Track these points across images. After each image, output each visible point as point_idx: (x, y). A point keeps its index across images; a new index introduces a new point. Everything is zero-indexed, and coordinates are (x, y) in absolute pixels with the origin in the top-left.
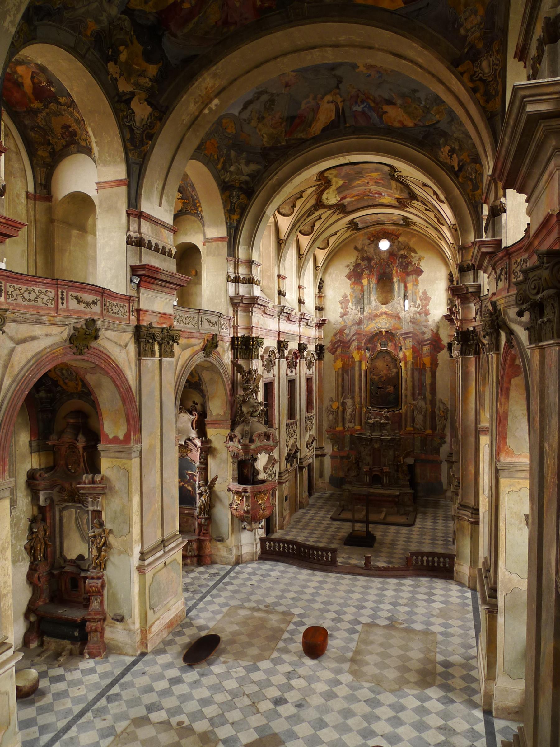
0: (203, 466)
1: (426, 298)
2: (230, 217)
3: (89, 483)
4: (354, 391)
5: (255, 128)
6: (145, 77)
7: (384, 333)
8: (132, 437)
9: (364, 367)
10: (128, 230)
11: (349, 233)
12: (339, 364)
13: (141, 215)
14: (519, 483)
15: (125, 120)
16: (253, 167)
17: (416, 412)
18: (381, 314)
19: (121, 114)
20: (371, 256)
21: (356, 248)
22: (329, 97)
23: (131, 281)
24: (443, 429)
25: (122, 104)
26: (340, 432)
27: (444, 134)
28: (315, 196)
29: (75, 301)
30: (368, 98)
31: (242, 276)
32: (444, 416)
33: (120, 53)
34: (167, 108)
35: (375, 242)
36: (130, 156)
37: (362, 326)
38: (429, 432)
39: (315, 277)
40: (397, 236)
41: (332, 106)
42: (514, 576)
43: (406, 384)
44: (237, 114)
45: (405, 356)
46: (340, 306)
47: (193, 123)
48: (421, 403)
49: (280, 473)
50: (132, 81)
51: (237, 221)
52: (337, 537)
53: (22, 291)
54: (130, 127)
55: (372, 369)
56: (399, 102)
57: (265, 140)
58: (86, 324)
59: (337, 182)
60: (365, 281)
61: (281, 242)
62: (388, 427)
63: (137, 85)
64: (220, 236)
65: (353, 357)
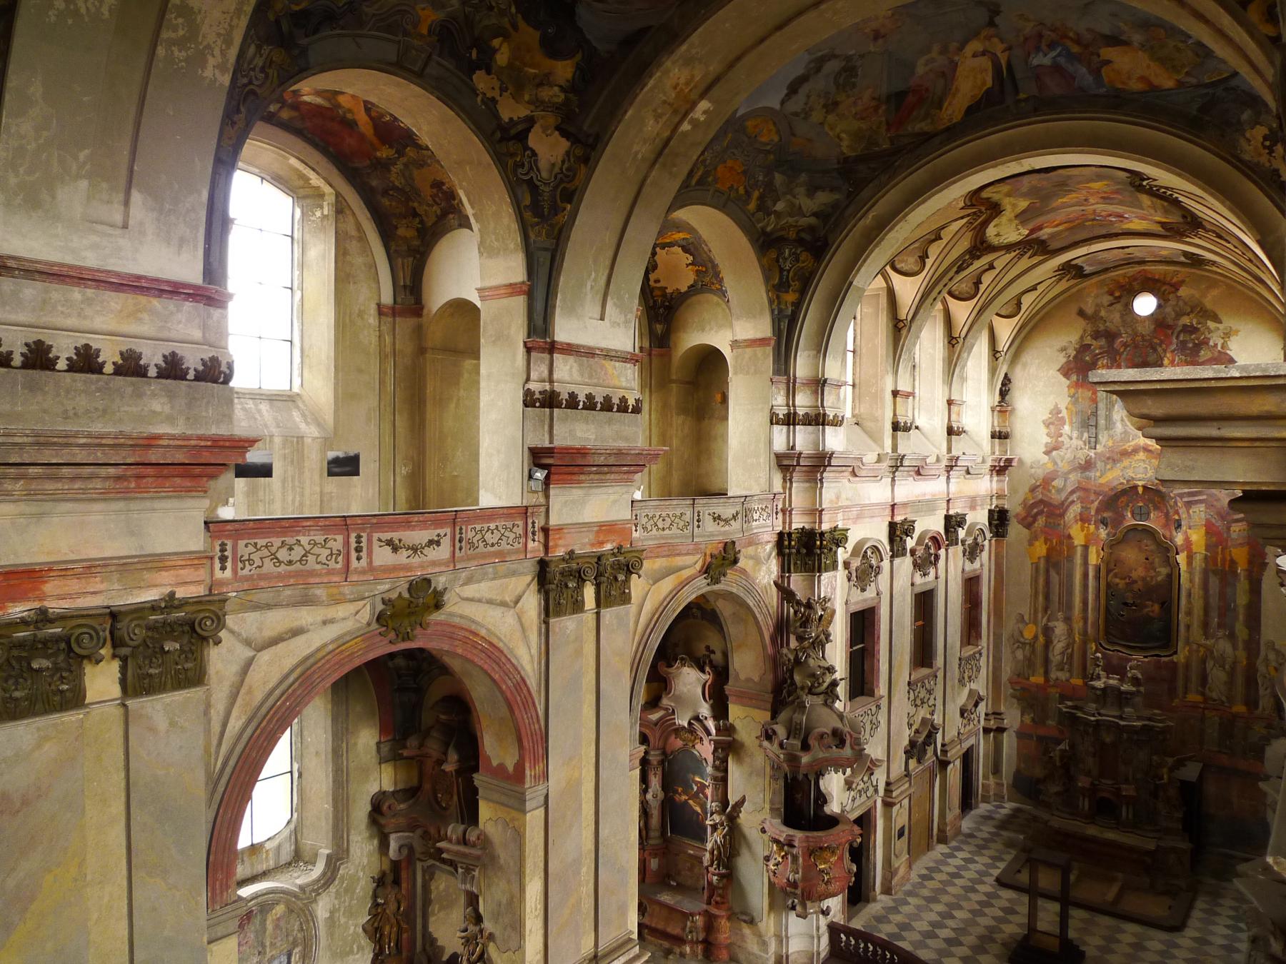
0: (720, 775)
2: (778, 297)
3: (458, 843)
4: (1070, 607)
5: (822, 124)
6: (551, 85)
7: (1140, 490)
8: (528, 772)
9: (1093, 559)
10: (528, 379)
11: (1064, 285)
12: (1041, 549)
13: (552, 348)
15: (520, 170)
16: (823, 198)
17: (1210, 664)
18: (1135, 451)
19: (511, 162)
21: (1081, 313)
23: (530, 477)
25: (511, 143)
26: (1037, 686)
28: (969, 235)
29: (388, 549)
30: (1066, 37)
31: (801, 412)
33: (495, 51)
34: (598, 138)
35: (1123, 300)
36: (532, 236)
37: (1092, 474)
38: (1240, 708)
39: (993, 371)
40: (1176, 286)
41: (985, 62)
43: (1189, 602)
44: (778, 107)
45: (1187, 540)
46: (1045, 431)
47: (660, 154)
48: (1224, 646)
49: (888, 784)
50: (527, 97)
51: (793, 304)
52: (998, 936)
53: (273, 549)
55: (1111, 564)
56: (1137, 38)
57: (845, 143)
58: (409, 590)
59: (1013, 205)
62: (1138, 699)
63: (537, 103)
64: (759, 335)
65: (1069, 537)
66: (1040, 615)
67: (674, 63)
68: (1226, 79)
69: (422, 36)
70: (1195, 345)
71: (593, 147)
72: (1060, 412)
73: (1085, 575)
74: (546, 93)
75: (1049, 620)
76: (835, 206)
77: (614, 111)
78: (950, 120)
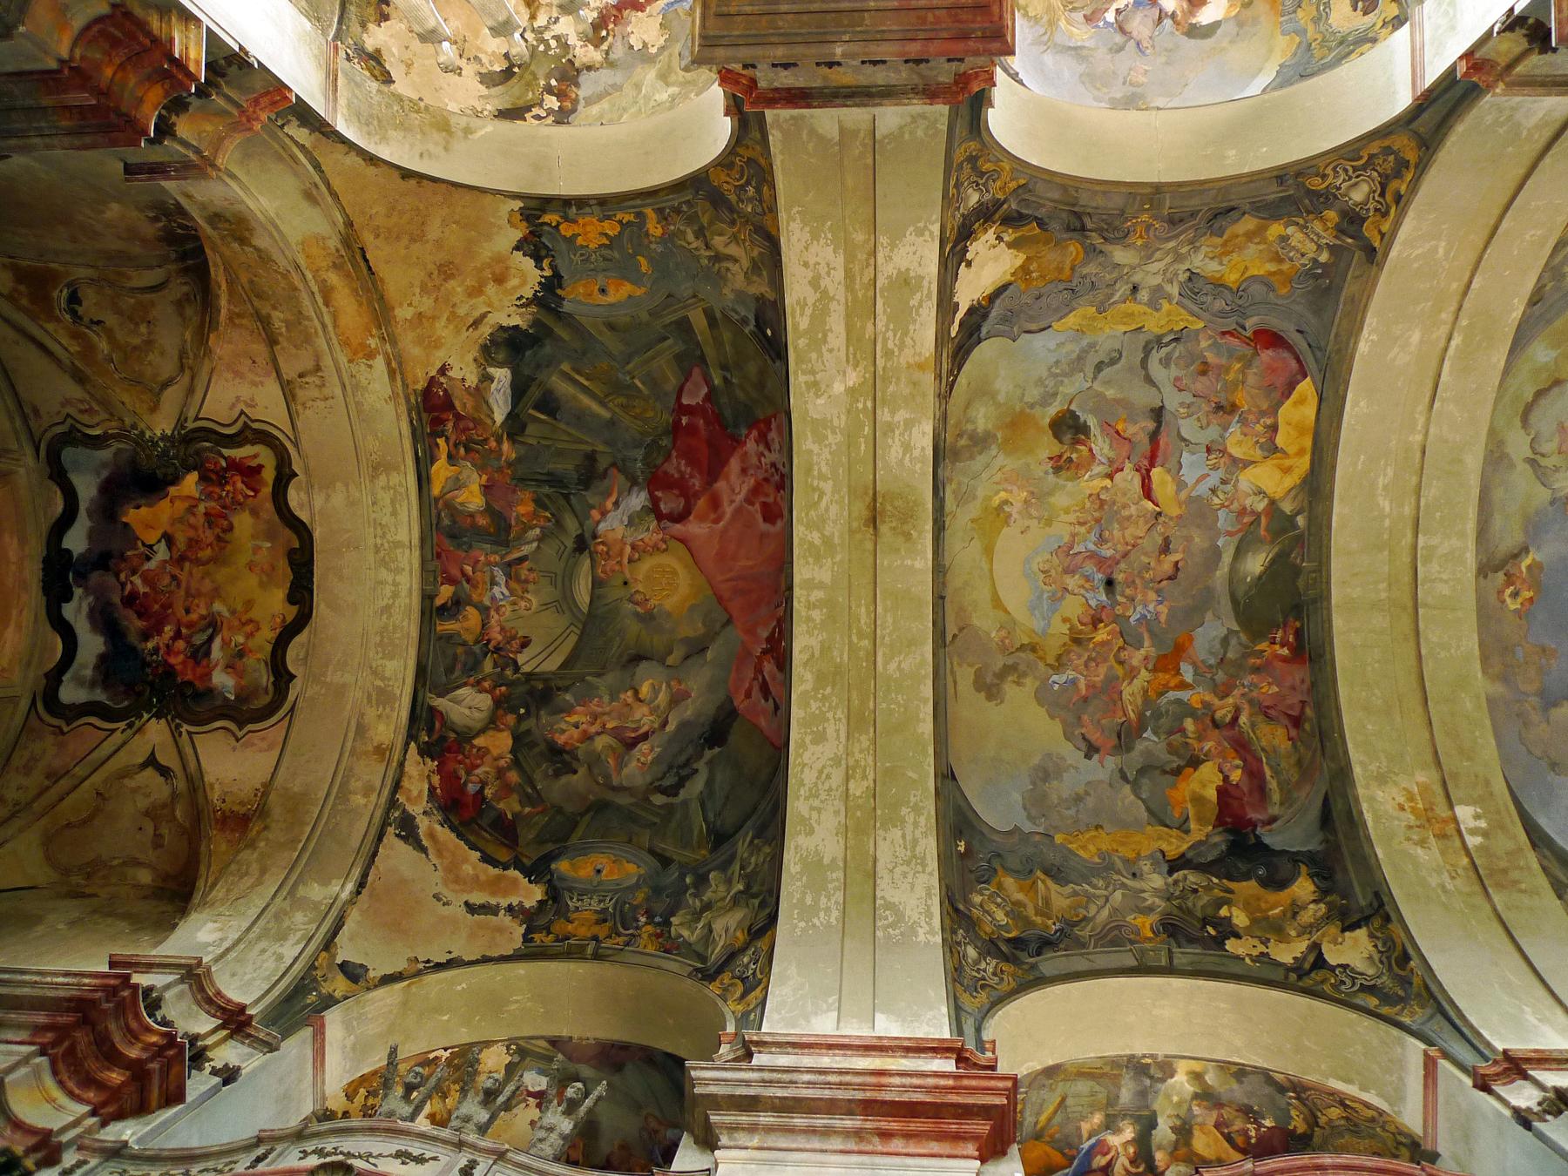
6: (1304, 908)
33: (1229, 919)
34: (1377, 895)
36: (1406, 1020)
50: (1293, 933)
54: (1363, 988)
67: (1367, 787)
69: (1150, 939)
71: (1382, 905)
74: (1307, 917)
77: (1367, 864)
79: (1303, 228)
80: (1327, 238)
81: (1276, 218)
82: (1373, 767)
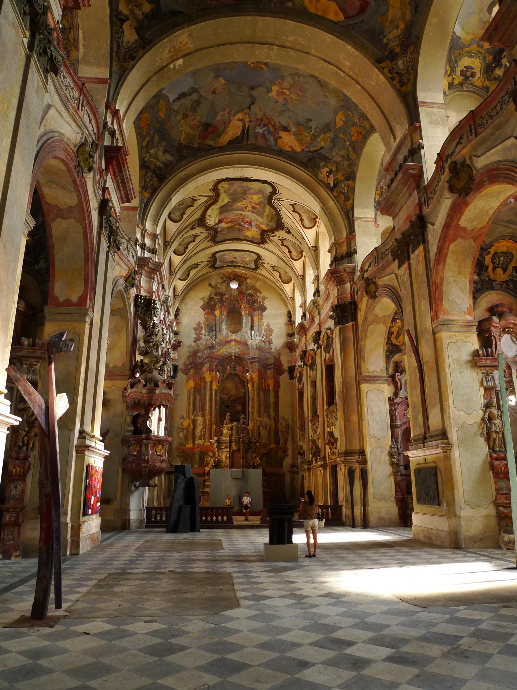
1: (269, 330)
2: (142, 192)
4: (204, 410)
5: (179, 122)
6: (140, 10)
7: (233, 357)
9: (214, 387)
12: (192, 384)
14: (456, 336)
16: (168, 157)
17: (261, 428)
18: (231, 341)
20: (223, 292)
21: (210, 285)
22: (240, 116)
24: (286, 443)
26: (190, 449)
27: (326, 159)
28: (203, 208)
32: (286, 431)
35: (227, 282)
38: (273, 446)
40: (246, 279)
41: (240, 124)
42: (462, 413)
45: (251, 377)
46: (194, 332)
48: (267, 420)
50: (130, 7)
55: (222, 390)
56: (293, 129)
57: (183, 137)
60: (217, 313)
61: (167, 244)
63: (132, 12)
65: (204, 378)
66: (191, 414)
68: (319, 150)
70: (253, 301)
72: (201, 324)
73: (211, 395)
74: (137, 12)
75: (195, 417)
76: (171, 162)
78: (222, 144)
79: (398, 37)
80: (391, 45)
81: (406, 28)
82: (195, 32)
